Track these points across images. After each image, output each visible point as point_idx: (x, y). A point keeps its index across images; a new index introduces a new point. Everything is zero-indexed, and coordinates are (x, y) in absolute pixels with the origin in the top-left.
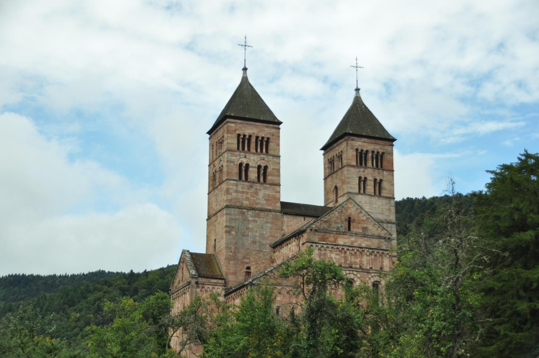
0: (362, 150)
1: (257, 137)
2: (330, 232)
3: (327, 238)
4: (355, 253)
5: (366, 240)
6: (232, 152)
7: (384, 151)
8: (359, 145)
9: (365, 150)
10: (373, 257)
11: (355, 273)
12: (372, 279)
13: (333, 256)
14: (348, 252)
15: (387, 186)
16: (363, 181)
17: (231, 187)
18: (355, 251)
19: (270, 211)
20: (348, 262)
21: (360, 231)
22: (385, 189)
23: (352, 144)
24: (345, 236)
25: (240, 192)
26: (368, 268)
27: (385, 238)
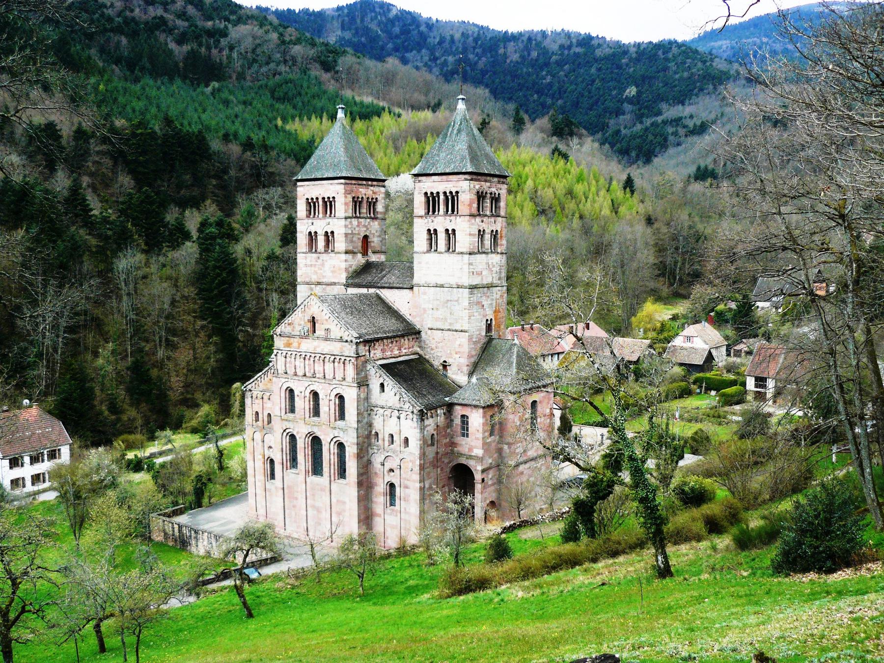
0: (432, 193)
1: (324, 198)
2: (293, 337)
8: (428, 187)
9: (435, 192)
13: (297, 363)
16: (432, 234)
19: (334, 284)
23: (420, 188)
27: (347, 341)
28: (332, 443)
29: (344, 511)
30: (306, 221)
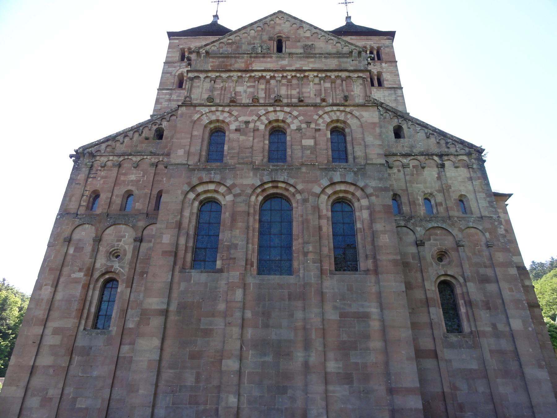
3: (231, 65)
4: (289, 81)
5: (312, 62)
6: (170, 64)
7: (380, 45)
10: (328, 85)
11: (287, 109)
12: (326, 116)
13: (239, 89)
14: (273, 82)
15: (389, 77)
17: (161, 97)
18: (289, 77)
20: (272, 96)
21: (301, 51)
22: (387, 80)
24: (269, 59)
25: (173, 100)
26: (318, 100)
28: (324, 198)
29: (367, 337)
30: (176, 64)
